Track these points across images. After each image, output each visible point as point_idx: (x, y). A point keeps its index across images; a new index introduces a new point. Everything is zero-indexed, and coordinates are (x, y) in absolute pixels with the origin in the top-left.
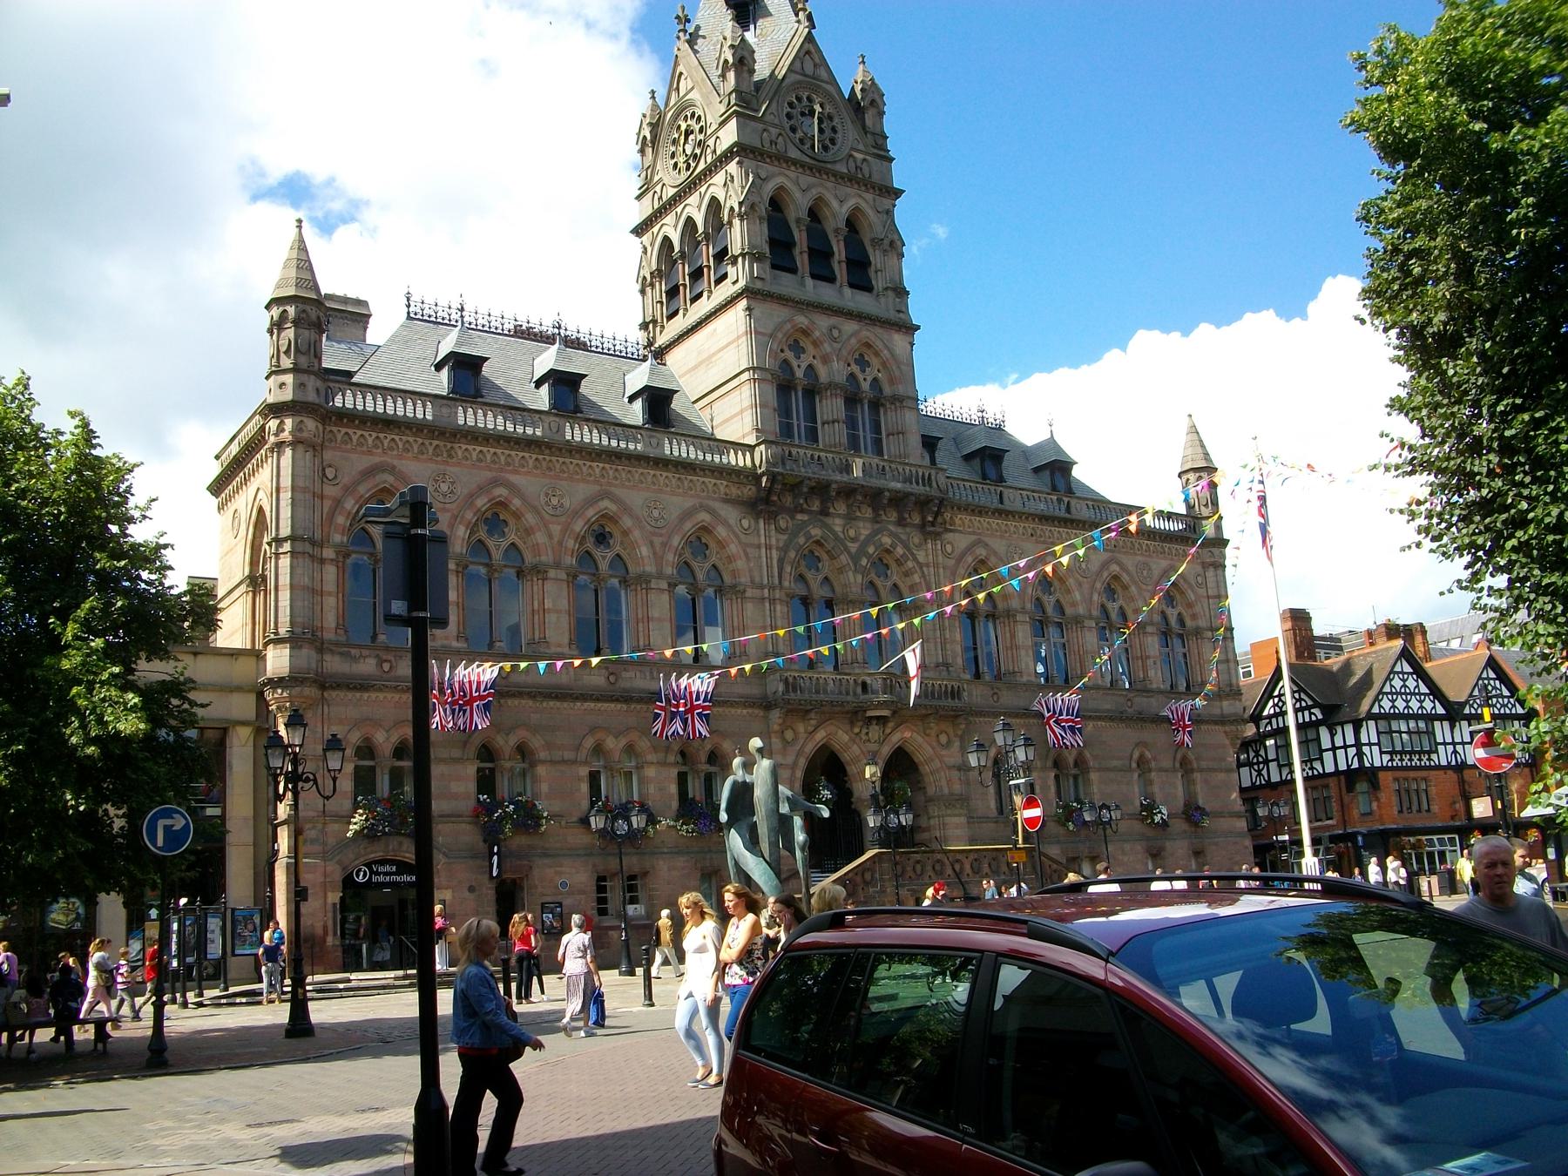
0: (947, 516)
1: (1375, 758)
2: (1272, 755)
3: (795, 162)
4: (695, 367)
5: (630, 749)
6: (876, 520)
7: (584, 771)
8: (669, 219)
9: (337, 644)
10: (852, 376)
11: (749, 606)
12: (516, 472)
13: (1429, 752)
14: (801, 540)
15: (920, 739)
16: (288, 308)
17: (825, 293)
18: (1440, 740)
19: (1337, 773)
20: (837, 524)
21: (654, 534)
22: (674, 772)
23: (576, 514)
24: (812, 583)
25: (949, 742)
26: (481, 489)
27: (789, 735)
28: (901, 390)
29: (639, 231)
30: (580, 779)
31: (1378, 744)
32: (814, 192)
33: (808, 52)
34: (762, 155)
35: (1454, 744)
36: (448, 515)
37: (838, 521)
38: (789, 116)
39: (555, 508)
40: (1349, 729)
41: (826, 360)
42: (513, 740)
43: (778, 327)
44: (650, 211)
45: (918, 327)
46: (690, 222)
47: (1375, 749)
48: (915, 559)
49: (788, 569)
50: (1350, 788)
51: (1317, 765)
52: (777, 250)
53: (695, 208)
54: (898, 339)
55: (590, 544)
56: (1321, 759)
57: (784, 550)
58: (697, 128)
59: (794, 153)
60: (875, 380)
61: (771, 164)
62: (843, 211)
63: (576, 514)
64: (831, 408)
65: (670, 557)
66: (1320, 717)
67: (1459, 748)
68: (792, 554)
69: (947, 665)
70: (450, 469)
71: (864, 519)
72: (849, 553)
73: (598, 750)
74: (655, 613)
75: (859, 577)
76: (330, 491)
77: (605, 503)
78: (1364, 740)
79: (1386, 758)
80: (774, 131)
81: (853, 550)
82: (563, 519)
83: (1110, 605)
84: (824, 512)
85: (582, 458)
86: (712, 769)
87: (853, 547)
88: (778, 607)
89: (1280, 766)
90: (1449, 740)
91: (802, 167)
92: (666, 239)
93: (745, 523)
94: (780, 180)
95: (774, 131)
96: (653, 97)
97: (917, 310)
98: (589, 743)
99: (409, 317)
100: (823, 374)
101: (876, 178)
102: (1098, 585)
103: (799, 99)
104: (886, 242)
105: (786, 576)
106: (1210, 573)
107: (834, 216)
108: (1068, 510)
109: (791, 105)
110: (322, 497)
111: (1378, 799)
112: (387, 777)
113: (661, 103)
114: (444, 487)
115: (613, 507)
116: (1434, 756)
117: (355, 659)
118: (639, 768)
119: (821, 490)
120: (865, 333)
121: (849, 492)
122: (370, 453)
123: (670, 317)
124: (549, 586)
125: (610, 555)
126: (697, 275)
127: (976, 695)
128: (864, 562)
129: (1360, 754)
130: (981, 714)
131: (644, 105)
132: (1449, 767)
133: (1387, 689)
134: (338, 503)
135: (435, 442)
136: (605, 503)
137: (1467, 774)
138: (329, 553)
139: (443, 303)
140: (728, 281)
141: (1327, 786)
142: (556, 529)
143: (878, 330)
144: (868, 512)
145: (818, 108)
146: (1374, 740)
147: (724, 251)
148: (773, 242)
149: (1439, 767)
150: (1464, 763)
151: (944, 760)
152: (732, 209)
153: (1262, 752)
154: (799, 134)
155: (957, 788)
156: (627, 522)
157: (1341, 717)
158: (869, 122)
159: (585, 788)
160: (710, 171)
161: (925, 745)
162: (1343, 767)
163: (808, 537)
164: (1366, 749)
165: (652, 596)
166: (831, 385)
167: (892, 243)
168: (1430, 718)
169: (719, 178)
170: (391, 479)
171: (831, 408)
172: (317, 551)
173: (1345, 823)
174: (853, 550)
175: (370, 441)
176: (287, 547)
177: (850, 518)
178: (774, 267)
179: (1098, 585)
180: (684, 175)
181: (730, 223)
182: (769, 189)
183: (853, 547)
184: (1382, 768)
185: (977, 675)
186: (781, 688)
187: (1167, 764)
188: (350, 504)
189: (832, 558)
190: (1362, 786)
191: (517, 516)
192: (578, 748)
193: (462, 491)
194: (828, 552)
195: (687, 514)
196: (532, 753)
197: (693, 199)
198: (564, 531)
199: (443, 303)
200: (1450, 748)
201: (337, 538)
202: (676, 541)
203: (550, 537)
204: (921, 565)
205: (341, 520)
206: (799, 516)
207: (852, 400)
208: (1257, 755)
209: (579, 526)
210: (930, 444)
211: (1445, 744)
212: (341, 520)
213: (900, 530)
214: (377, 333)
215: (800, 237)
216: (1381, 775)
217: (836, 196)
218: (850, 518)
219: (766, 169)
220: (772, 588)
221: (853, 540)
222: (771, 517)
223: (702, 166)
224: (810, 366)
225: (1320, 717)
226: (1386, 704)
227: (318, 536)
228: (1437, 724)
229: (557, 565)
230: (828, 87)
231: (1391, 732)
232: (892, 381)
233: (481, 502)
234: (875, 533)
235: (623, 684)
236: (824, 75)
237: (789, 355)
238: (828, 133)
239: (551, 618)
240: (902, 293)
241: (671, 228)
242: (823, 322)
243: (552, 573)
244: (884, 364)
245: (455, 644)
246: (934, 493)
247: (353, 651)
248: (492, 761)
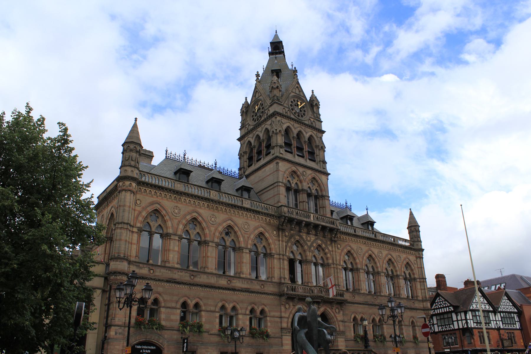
0: (339, 235)
1: (472, 324)
2: (435, 322)
3: (293, 119)
4: (258, 182)
5: (234, 308)
6: (316, 235)
7: (218, 315)
8: (251, 135)
9: (135, 262)
10: (309, 187)
11: (276, 261)
12: (200, 208)
13: (489, 323)
14: (293, 240)
15: (330, 310)
16: (130, 145)
17: (301, 161)
18: (491, 319)
19: (459, 329)
20: (304, 236)
21: (245, 234)
22: (248, 317)
23: (220, 224)
24: (295, 254)
25: (339, 312)
26: (189, 213)
27: (287, 306)
28: (324, 194)
29: (239, 140)
30: (216, 317)
31: (473, 319)
32: (299, 129)
33: (297, 87)
34: (283, 116)
35: (496, 321)
36: (177, 221)
37: (304, 234)
38: (291, 105)
39: (213, 222)
40: (463, 314)
41: (301, 182)
42: (194, 302)
43: (287, 170)
44: (244, 133)
45: (330, 174)
46: (258, 136)
47: (472, 321)
48: (328, 249)
49: (288, 249)
50: (464, 335)
51: (452, 326)
52: (288, 145)
53: (260, 132)
54: (323, 177)
55: (224, 235)
56: (453, 324)
57: (287, 242)
58: (261, 108)
59: (292, 116)
60: (316, 189)
61: (286, 119)
62: (307, 136)
63: (220, 224)
64: (303, 197)
65: (250, 242)
66: (452, 310)
67: (498, 322)
68: (290, 244)
69: (339, 285)
70: (179, 205)
71: (313, 234)
72: (308, 245)
73: (223, 307)
74: (244, 261)
75: (311, 253)
76: (138, 208)
77: (229, 222)
78: (468, 318)
79: (475, 324)
80: (287, 109)
81: (309, 244)
82: (215, 226)
83: (388, 269)
84: (300, 231)
85: (223, 206)
86: (261, 317)
87: (309, 244)
88: (285, 262)
89: (438, 326)
90: (494, 319)
91: (295, 121)
92: (249, 142)
93: (275, 232)
94: (288, 124)
95: (287, 109)
96: (246, 99)
97: (329, 168)
98: (220, 305)
99: (166, 157)
100: (300, 188)
101: (317, 127)
102: (385, 262)
103: (294, 101)
104: (320, 147)
105: (287, 251)
106: (418, 260)
107: (304, 137)
108: (375, 236)
109: (292, 102)
110: (135, 210)
111: (474, 339)
112: (149, 312)
113: (249, 102)
114: (176, 211)
115: (232, 223)
116: (490, 325)
117: (141, 268)
118: (237, 314)
119: (299, 223)
120: (313, 174)
121: (308, 224)
122: (152, 196)
123: (249, 166)
124: (210, 248)
125: (230, 239)
126: (259, 153)
127: (347, 296)
128: (312, 248)
129: (467, 323)
130: (349, 303)
131: (243, 101)
132: (495, 329)
133: (474, 301)
134: (140, 213)
135: (175, 196)
136: (229, 222)
137: (501, 331)
138: (135, 230)
139: (178, 154)
140: (271, 154)
141: (455, 334)
142: (213, 229)
143: (317, 174)
144: (314, 232)
146: (471, 318)
147: (270, 145)
148: (285, 143)
149: (492, 329)
150: (500, 327)
151: (338, 316)
152: (273, 131)
153: (432, 321)
154: (294, 111)
155: (342, 328)
156: (236, 229)
157: (460, 310)
158: (315, 110)
159: (218, 320)
160: (266, 120)
161: (331, 313)
162: (461, 327)
163: (295, 239)
164: (469, 321)
165: (244, 254)
166: (303, 190)
167: (322, 147)
168: (488, 312)
169: (269, 122)
170: (159, 206)
171: (303, 197)
172: (131, 229)
173: (462, 346)
174: (309, 244)
175: (153, 193)
176: (120, 226)
177: (308, 233)
178: (286, 151)
179: (385, 262)
180: (257, 122)
181: (272, 136)
182: (285, 127)
183: (309, 244)
184: (474, 328)
185: (347, 289)
186: (286, 289)
187: (407, 323)
188: (144, 214)
189: (302, 246)
190: (467, 334)
191: (200, 223)
192: (216, 306)
193: (182, 213)
194: (301, 245)
195: (256, 228)
196: (200, 307)
197: (259, 129)
198: (216, 230)
199: (178, 154)
200: (495, 322)
201: (138, 225)
202: (252, 236)
203: (210, 231)
204: (330, 251)
205: (140, 219)
206: (292, 232)
207: (309, 195)
208: (430, 322)
209: (220, 228)
210: (332, 212)
211: (493, 321)
212: (140, 219)
213: (324, 239)
214: (155, 162)
215: (294, 143)
216: (474, 330)
217: (305, 131)
218: (308, 233)
219: (284, 120)
220: (283, 255)
221: (309, 241)
222: (283, 230)
223: (263, 119)
224: (296, 183)
225: (452, 310)
226: (474, 306)
227: (132, 224)
228: (490, 314)
229: (212, 242)
231: (476, 316)
232: (321, 190)
233: (189, 217)
234: (316, 239)
235: (233, 285)
236: (302, 94)
237: (290, 179)
238: (303, 112)
239: (210, 259)
240: (325, 162)
241: (251, 138)
242: (301, 169)
243: (210, 244)
244: (319, 185)
245: (176, 266)
246: (335, 227)
247: (141, 265)
248: (186, 308)
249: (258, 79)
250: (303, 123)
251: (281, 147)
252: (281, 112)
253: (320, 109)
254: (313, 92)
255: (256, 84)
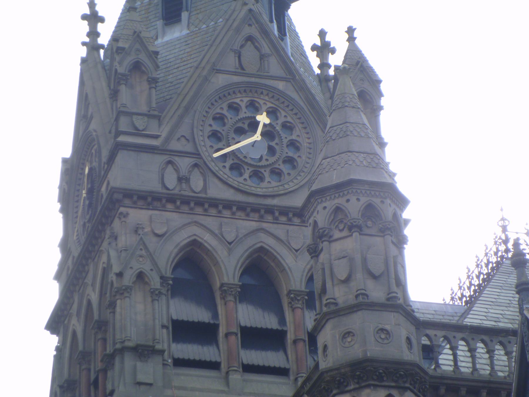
32: (251, 243)
33: (250, 39)
59: (217, 191)
61: (177, 210)
80: (184, 163)
109: (220, 118)
145: (263, 119)
178: (179, 363)
230: (281, 85)
249: (93, 34)
250: (270, 210)
251: (144, 351)
252: (154, 186)
253: (384, 117)
254: (351, 39)
255: (84, 61)
